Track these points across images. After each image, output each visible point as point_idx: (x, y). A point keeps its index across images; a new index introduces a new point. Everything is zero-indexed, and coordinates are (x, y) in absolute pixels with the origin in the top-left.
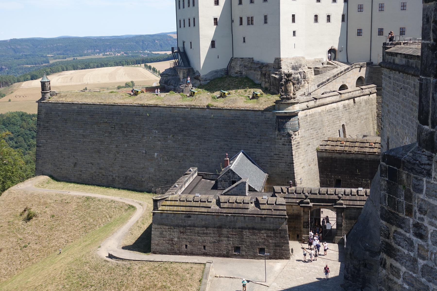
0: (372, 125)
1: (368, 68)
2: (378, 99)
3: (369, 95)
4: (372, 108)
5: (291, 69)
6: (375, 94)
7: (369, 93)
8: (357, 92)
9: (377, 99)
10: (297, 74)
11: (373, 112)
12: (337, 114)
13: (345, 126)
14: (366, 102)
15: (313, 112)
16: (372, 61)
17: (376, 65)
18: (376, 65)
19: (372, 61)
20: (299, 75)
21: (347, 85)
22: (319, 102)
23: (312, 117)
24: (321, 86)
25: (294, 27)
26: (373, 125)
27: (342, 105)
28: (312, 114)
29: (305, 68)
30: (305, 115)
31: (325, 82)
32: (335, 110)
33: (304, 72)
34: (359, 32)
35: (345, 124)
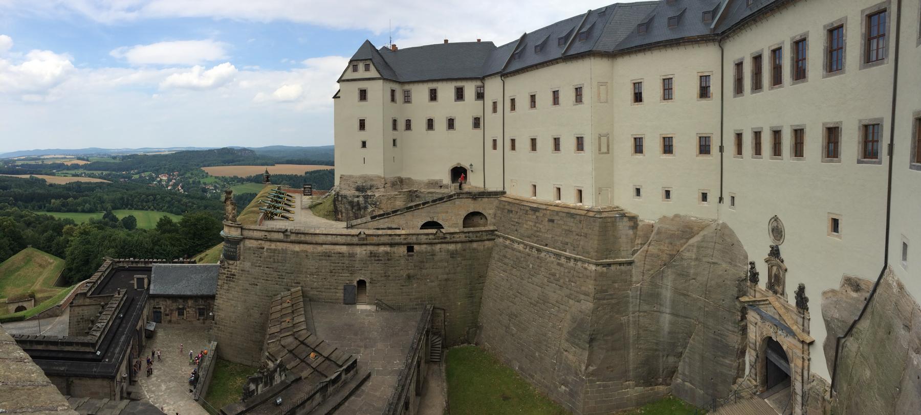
5: (354, 189)
10: (358, 197)
12: (347, 262)
13: (367, 284)
14: (453, 254)
15: (280, 248)
20: (361, 199)
21: (440, 222)
22: (293, 237)
23: (274, 253)
24: (378, 218)
25: (363, 136)
27: (364, 252)
28: (275, 250)
29: (379, 191)
30: (259, 246)
31: (388, 214)
32: (343, 257)
33: (374, 196)
35: (368, 281)
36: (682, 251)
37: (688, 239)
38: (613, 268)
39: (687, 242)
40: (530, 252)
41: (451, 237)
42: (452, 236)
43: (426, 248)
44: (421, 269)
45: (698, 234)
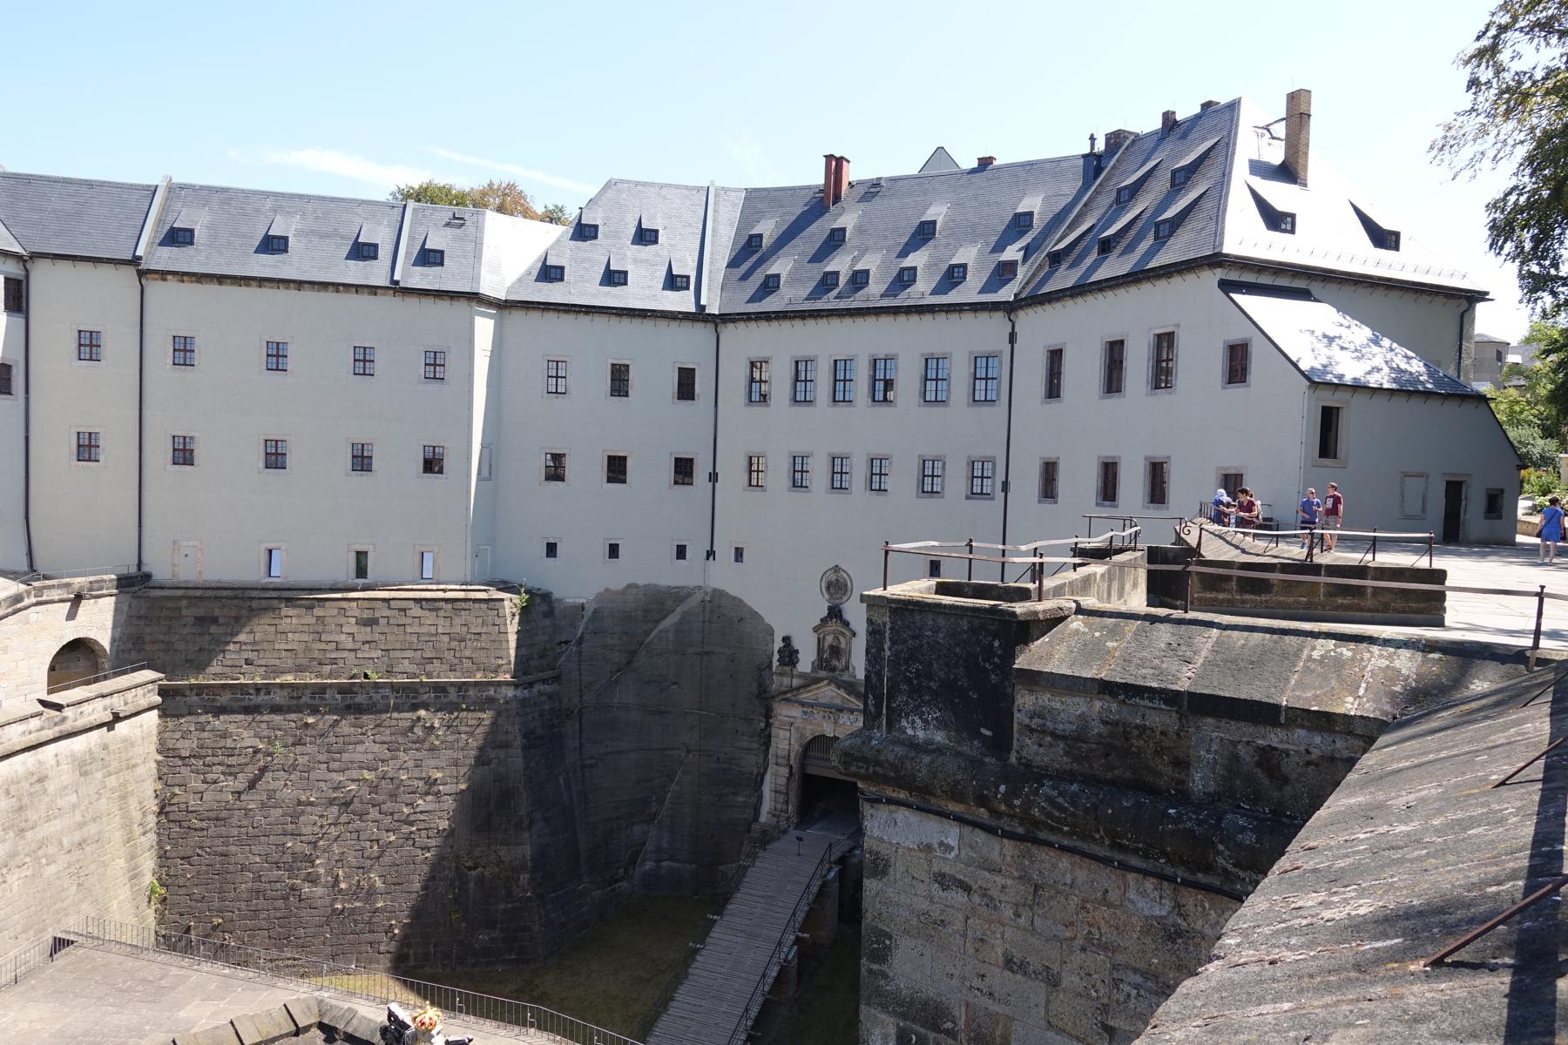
0: (121, 862)
1: (127, 598)
2: (167, 735)
3: (110, 725)
4: (124, 784)
6: (155, 712)
7: (111, 718)
8: (17, 729)
9: (159, 733)
11: (133, 804)
14: (83, 767)
16: (145, 569)
17: (162, 588)
18: (162, 588)
19: (145, 569)
26: (132, 857)
34: (87, 449)
36: (649, 643)
37: (658, 622)
38: (536, 689)
39: (655, 627)
40: (317, 702)
41: (75, 714)
42: (80, 710)
43: (24, 763)
44: (22, 830)
45: (673, 611)
